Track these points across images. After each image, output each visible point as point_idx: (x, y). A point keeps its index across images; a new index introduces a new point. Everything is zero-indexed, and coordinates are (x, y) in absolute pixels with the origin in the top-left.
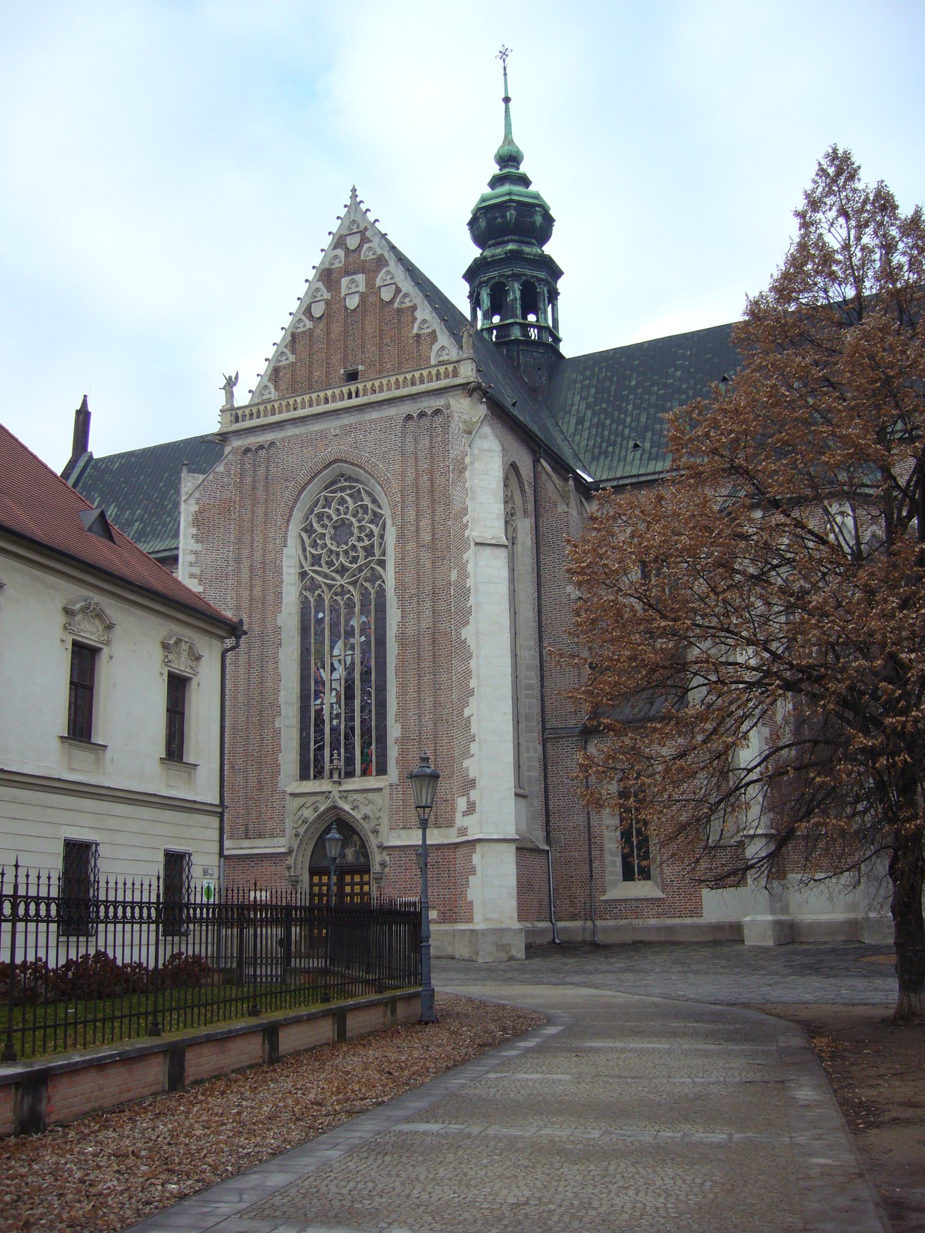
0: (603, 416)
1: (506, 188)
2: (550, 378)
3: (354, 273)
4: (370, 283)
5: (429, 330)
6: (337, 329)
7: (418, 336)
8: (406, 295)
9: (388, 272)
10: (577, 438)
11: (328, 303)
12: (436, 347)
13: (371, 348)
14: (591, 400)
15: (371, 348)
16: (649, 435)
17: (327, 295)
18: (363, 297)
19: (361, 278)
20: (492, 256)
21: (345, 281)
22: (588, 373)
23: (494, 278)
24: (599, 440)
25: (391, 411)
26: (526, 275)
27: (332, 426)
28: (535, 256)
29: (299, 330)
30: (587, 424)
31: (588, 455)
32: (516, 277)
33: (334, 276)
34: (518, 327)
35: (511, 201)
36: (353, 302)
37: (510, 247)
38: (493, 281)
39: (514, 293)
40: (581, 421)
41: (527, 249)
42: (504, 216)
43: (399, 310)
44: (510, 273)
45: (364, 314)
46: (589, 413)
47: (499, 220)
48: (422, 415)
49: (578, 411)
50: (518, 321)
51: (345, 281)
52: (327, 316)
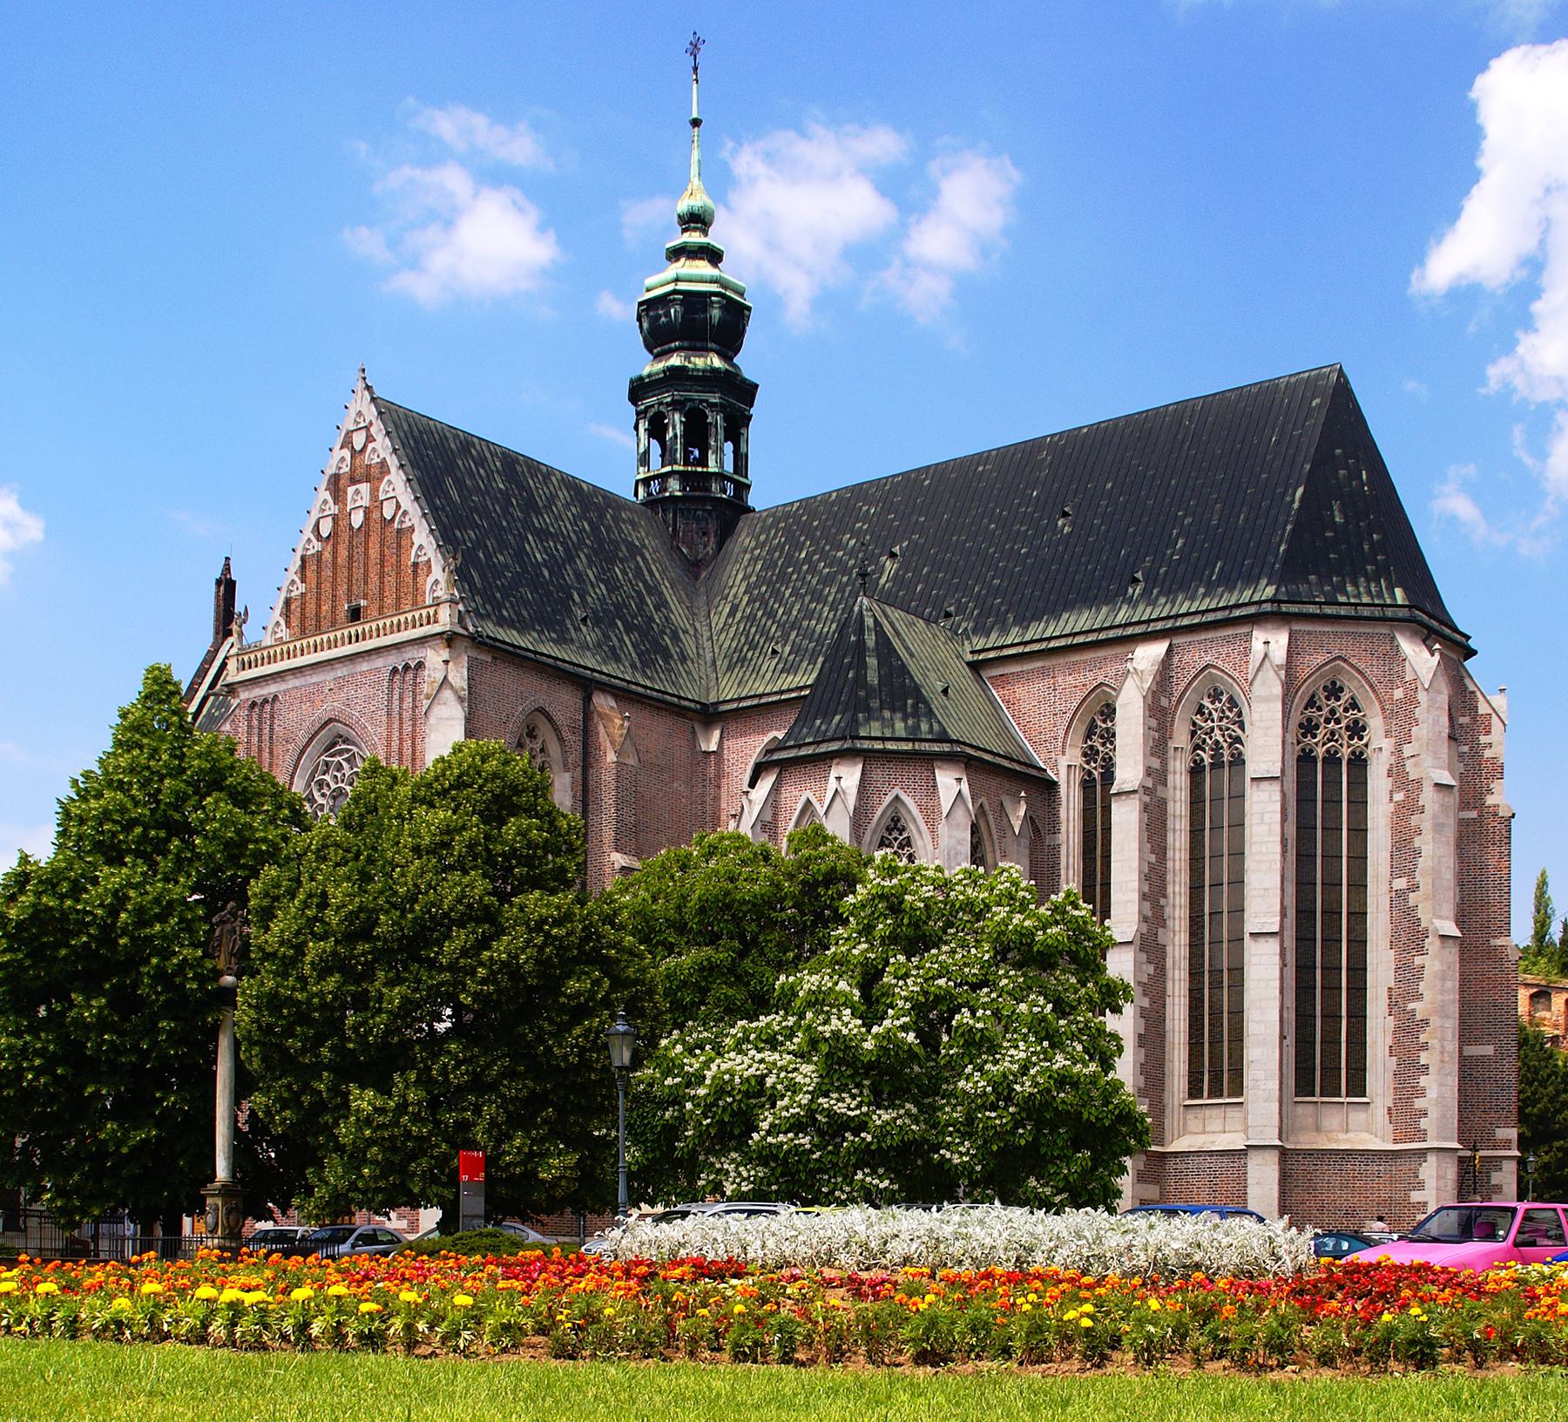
0: (757, 604)
1: (685, 267)
2: (720, 545)
3: (359, 482)
4: (374, 493)
5: (426, 558)
6: (343, 553)
7: (416, 565)
8: (405, 513)
9: (390, 482)
10: (723, 636)
11: (335, 519)
12: (430, 580)
13: (374, 578)
14: (754, 579)
15: (374, 578)
16: (794, 634)
17: (334, 509)
18: (367, 512)
19: (364, 488)
20: (649, 376)
21: (351, 490)
22: (762, 538)
23: (653, 406)
24: (743, 641)
25: (379, 662)
26: (693, 400)
27: (326, 677)
28: (704, 371)
29: (309, 553)
30: (739, 615)
31: (726, 662)
32: (676, 405)
33: (342, 482)
34: (677, 476)
35: (675, 292)
36: (357, 519)
37: (676, 360)
38: (650, 414)
39: (674, 428)
40: (732, 613)
41: (699, 362)
42: (667, 315)
43: (399, 531)
44: (669, 399)
45: (367, 536)
46: (746, 599)
47: (663, 319)
48: (407, 667)
49: (735, 596)
50: (676, 468)
51: (351, 490)
52: (334, 535)
